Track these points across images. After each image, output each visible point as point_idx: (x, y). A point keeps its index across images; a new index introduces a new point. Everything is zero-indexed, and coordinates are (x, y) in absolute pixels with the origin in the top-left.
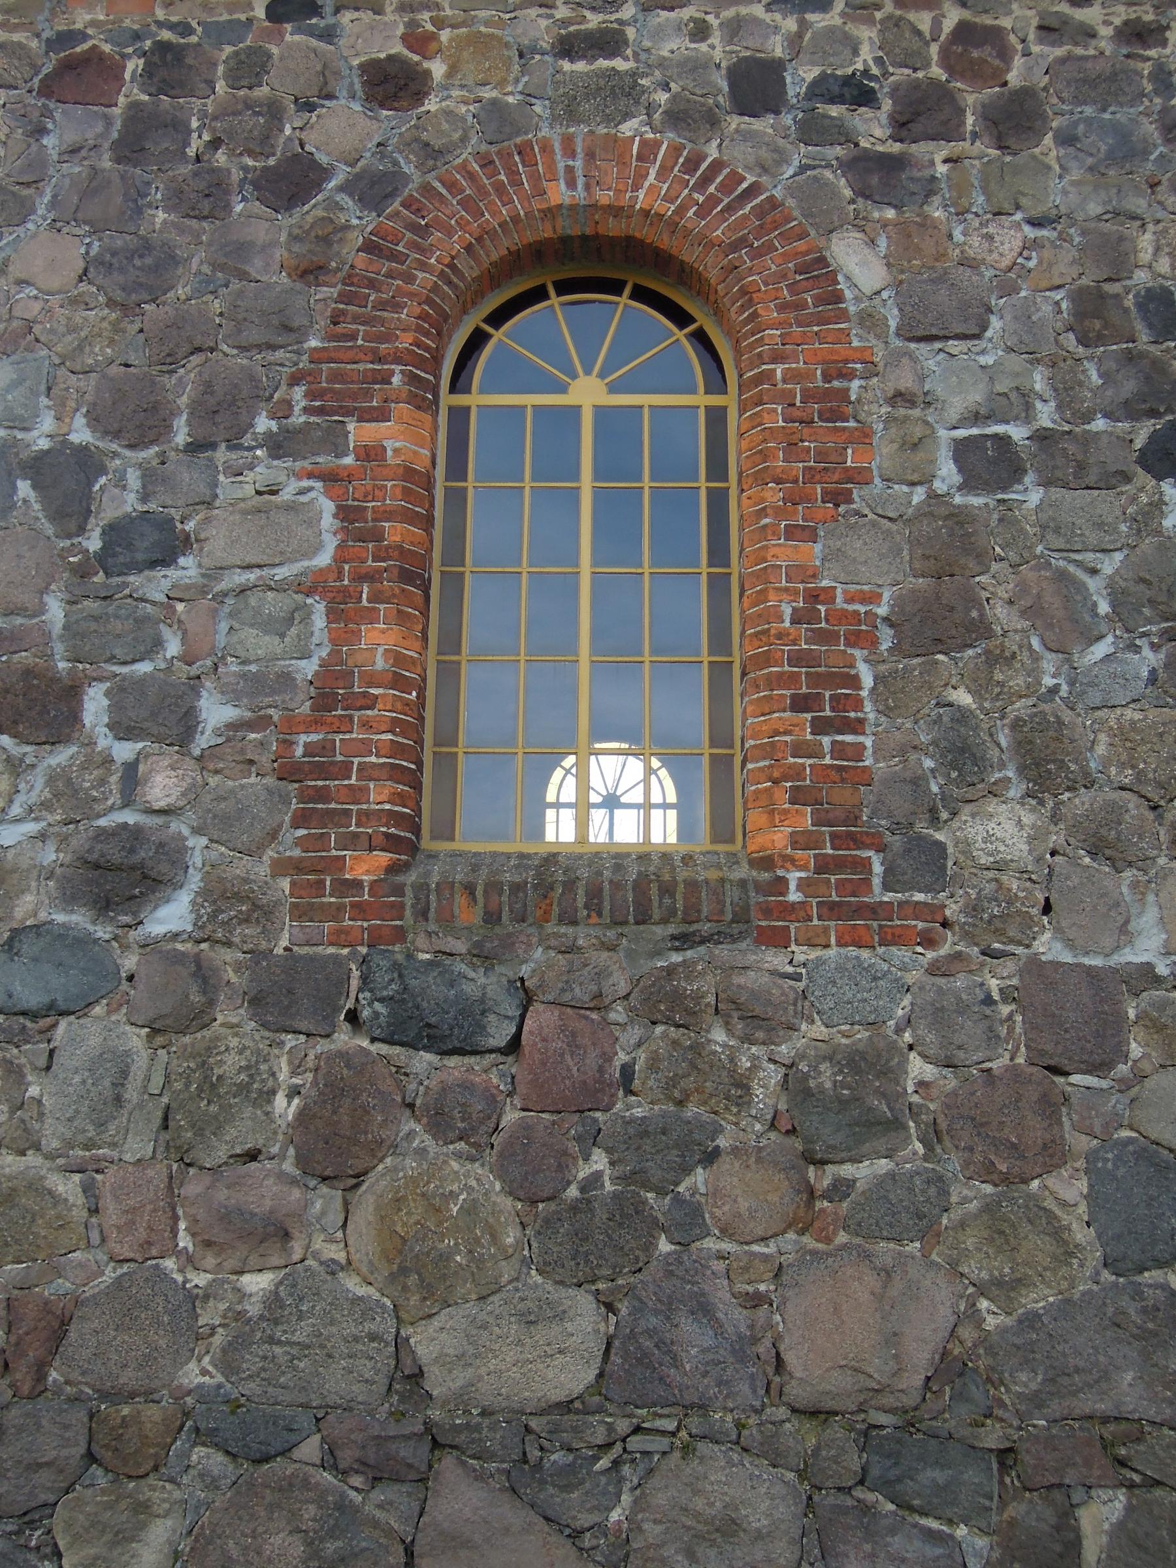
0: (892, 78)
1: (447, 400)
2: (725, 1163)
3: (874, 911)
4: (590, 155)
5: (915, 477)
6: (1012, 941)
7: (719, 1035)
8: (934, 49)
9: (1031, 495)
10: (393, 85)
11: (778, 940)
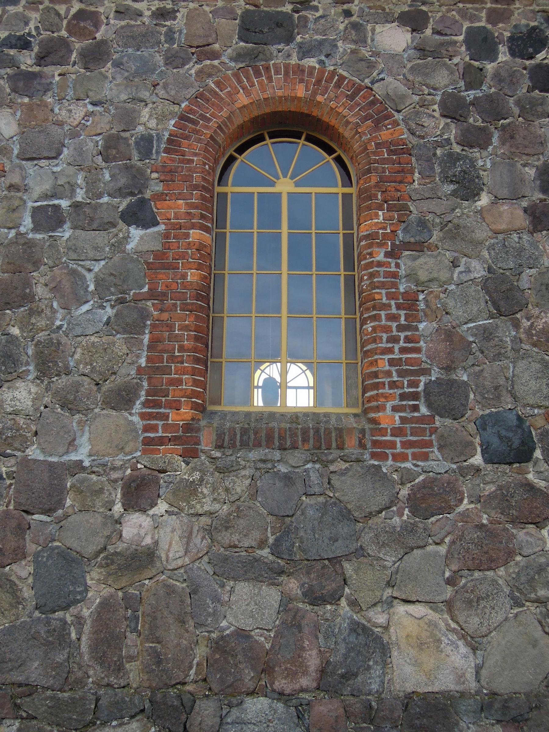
0: (41, 36)
5: (11, 225)
6: (16, 449)
8: (65, 22)
9: (66, 233)
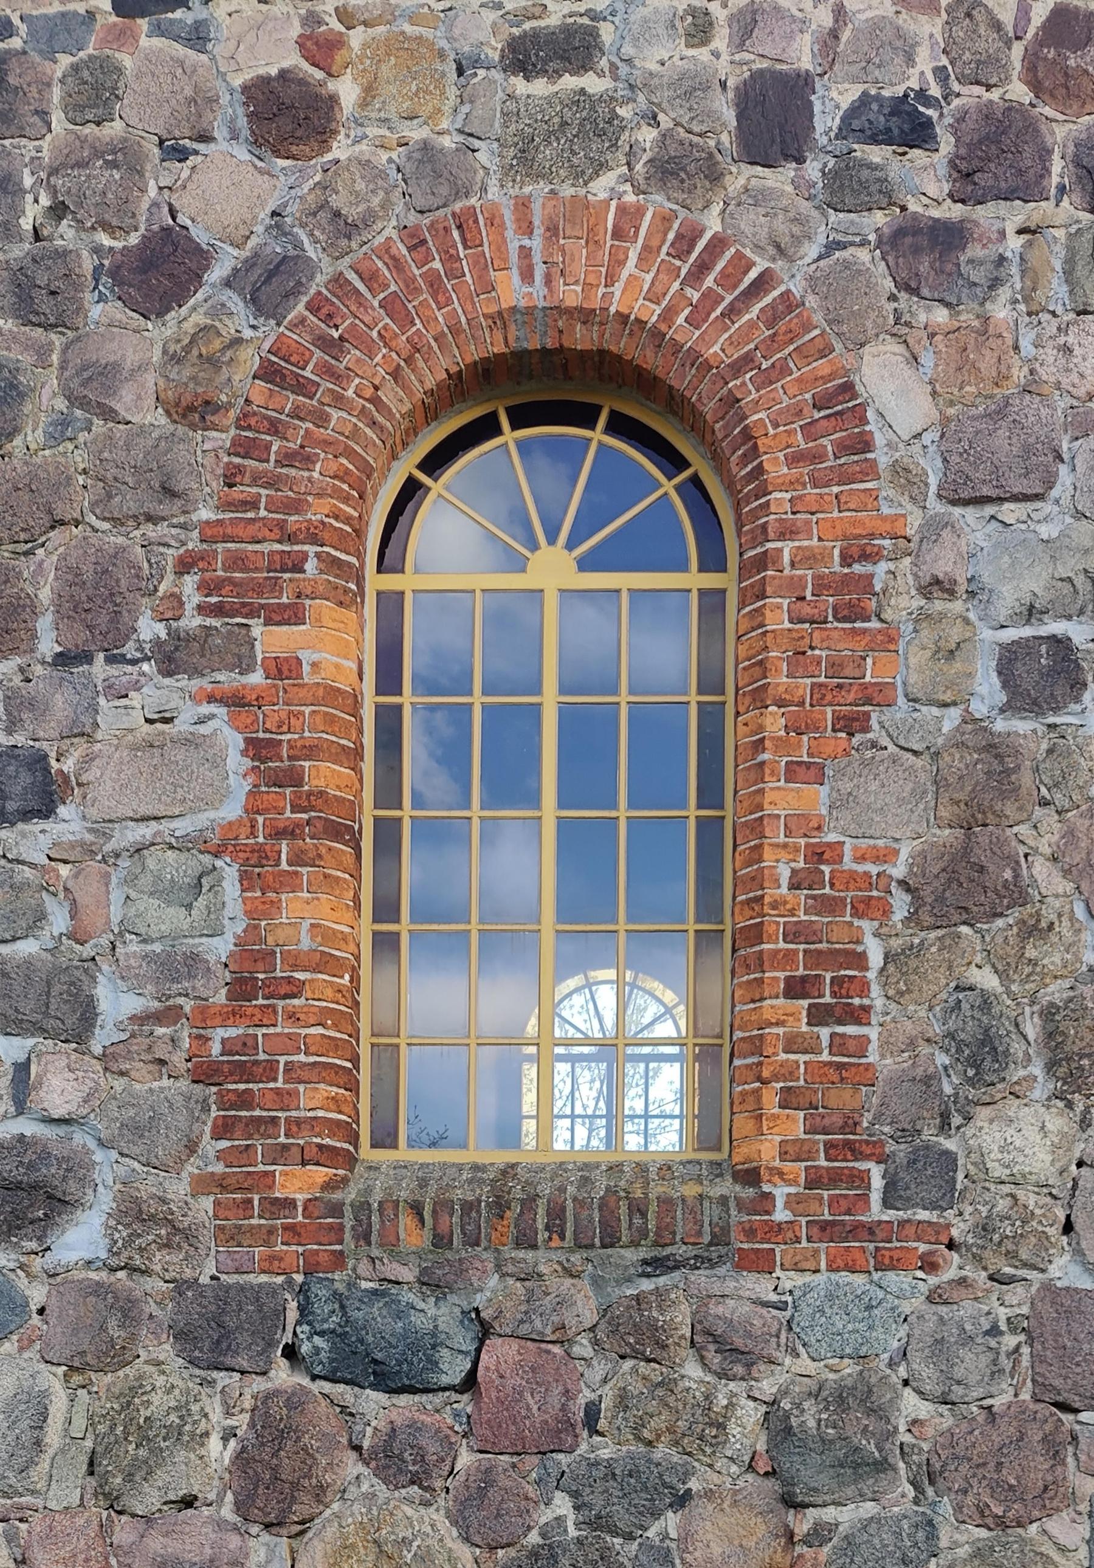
0: (956, 102)
1: (375, 582)
2: (701, 1508)
3: (870, 1230)
4: (552, 231)
5: (947, 697)
6: (1025, 1265)
7: (693, 1370)
8: (1017, 50)
10: (287, 116)
11: (762, 1263)
